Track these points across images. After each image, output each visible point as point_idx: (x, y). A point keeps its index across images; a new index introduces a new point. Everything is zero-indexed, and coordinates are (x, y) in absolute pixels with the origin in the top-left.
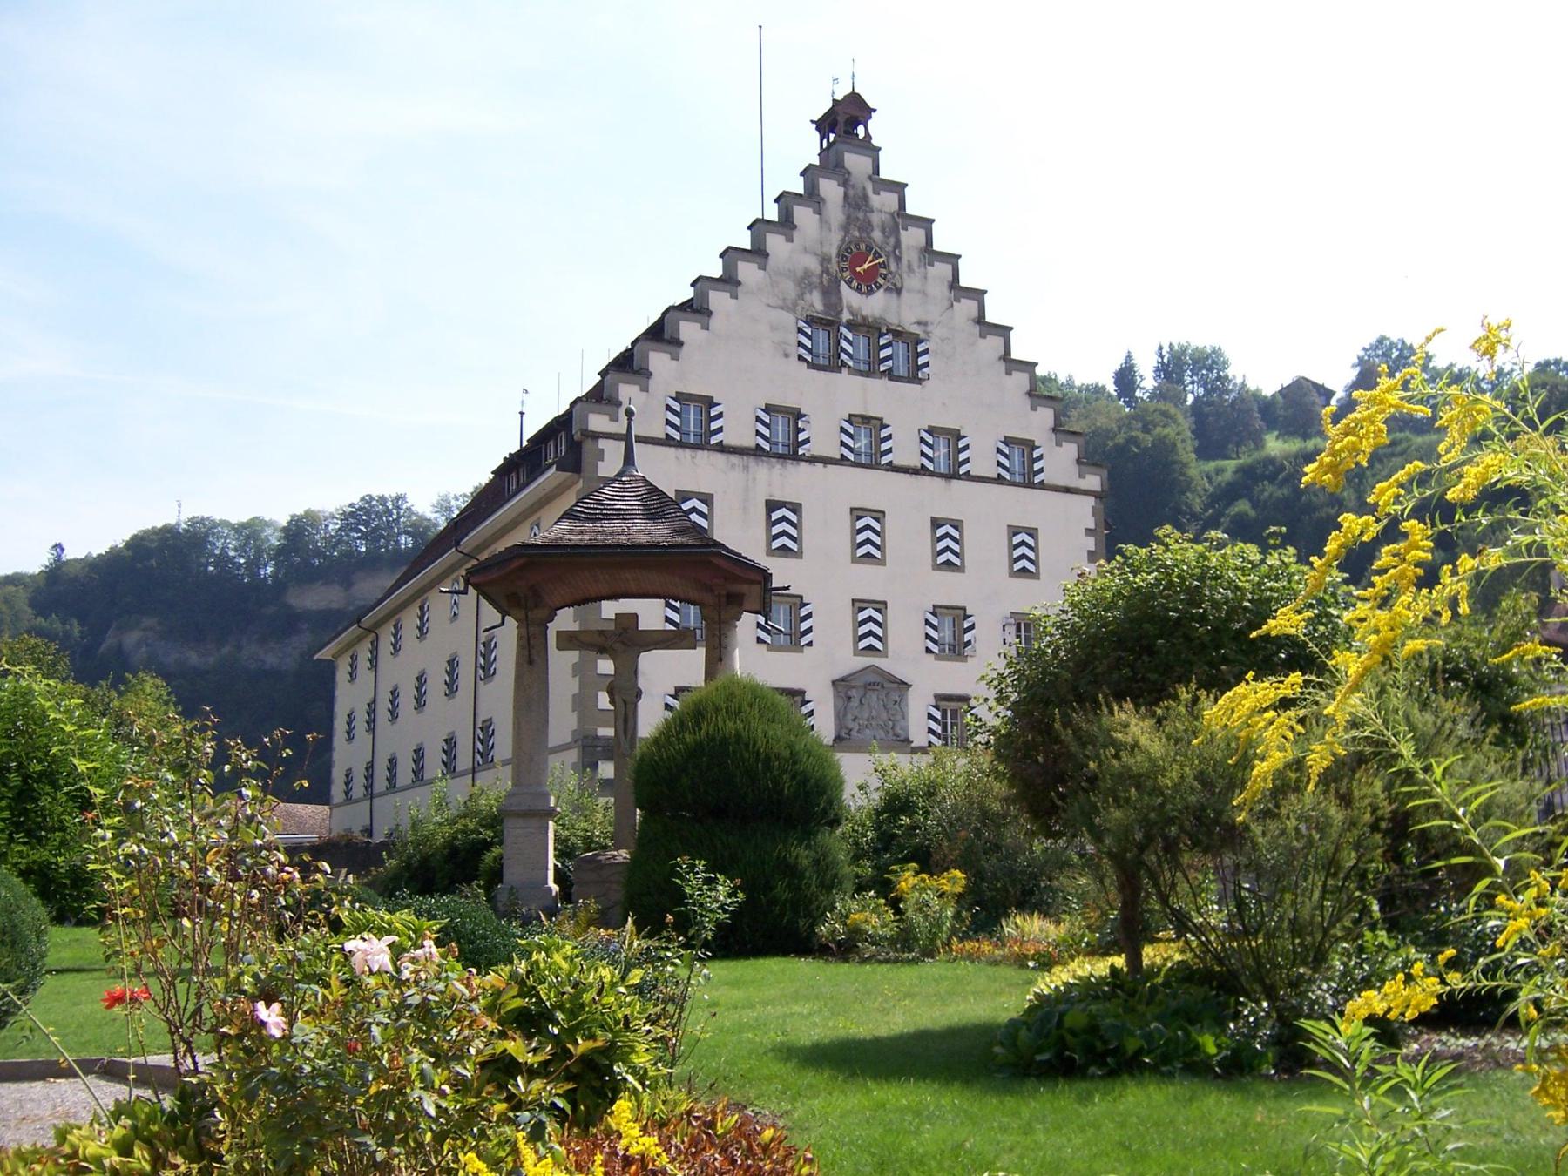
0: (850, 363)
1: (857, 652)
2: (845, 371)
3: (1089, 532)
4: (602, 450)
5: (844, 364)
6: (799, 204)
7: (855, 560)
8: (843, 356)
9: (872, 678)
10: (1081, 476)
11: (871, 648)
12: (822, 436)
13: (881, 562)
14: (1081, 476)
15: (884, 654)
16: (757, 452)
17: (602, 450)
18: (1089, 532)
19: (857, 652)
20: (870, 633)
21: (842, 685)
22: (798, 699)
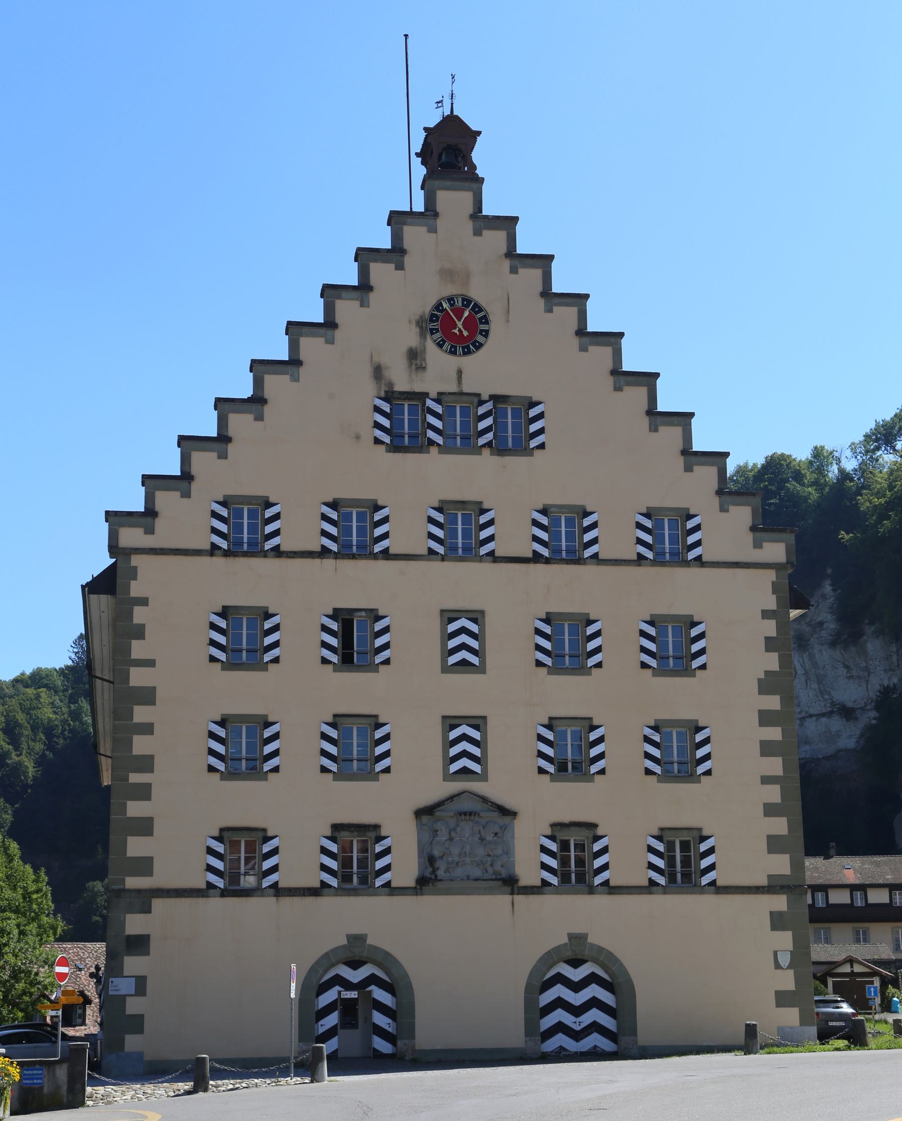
0: (439, 440)
1: (448, 777)
2: (434, 450)
3: (766, 614)
4: (136, 568)
5: (431, 442)
6: (376, 261)
7: (446, 669)
8: (431, 434)
10: (757, 545)
11: (465, 771)
13: (481, 669)
14: (757, 545)
15: (483, 777)
16: (324, 552)
17: (136, 568)
18: (766, 614)
19: (448, 777)
20: (464, 754)
22: (372, 835)
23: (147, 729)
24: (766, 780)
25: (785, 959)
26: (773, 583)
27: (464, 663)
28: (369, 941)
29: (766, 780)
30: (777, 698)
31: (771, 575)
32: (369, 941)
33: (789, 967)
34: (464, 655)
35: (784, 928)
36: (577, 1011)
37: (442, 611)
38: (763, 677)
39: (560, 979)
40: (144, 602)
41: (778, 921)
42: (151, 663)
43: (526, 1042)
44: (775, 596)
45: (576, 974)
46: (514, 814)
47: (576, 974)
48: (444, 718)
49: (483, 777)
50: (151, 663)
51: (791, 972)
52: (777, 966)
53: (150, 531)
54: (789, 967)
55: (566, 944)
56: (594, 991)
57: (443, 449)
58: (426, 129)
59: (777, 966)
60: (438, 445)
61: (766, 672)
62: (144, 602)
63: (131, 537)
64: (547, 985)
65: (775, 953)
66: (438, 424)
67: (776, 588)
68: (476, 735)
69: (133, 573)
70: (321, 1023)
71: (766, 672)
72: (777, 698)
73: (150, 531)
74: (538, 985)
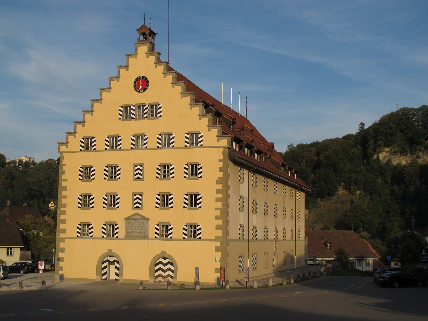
0: (134, 117)
2: (133, 120)
3: (220, 161)
4: (64, 156)
5: (132, 118)
7: (134, 180)
9: (137, 217)
10: (219, 140)
11: (137, 207)
12: (126, 143)
13: (143, 180)
14: (219, 140)
15: (142, 209)
18: (220, 161)
19: (133, 209)
20: (138, 203)
21: (127, 219)
23: (65, 197)
24: (217, 209)
25: (218, 260)
26: (222, 151)
27: (138, 178)
28: (113, 251)
29: (217, 209)
30: (221, 185)
31: (222, 149)
32: (113, 251)
33: (219, 262)
34: (138, 176)
35: (219, 251)
36: (164, 271)
37: (133, 164)
38: (218, 179)
39: (161, 263)
40: (65, 165)
41: (217, 249)
42: (66, 180)
43: (149, 279)
44: (223, 155)
45: (165, 262)
46: (149, 219)
47: (165, 262)
48: (133, 193)
49: (142, 209)
50: (66, 180)
51: (220, 263)
52: (216, 261)
53: (67, 147)
54: (219, 262)
55: (160, 254)
56: (169, 266)
57: (136, 119)
58: (137, 30)
59: (216, 261)
60: (134, 118)
61: (219, 178)
62: (65, 165)
63: (63, 149)
64: (157, 264)
65: (216, 258)
66: (134, 112)
67: (223, 153)
68: (140, 197)
69: (63, 158)
70: (103, 271)
71: (219, 178)
72: (221, 185)
73: (67, 147)
74: (154, 264)
